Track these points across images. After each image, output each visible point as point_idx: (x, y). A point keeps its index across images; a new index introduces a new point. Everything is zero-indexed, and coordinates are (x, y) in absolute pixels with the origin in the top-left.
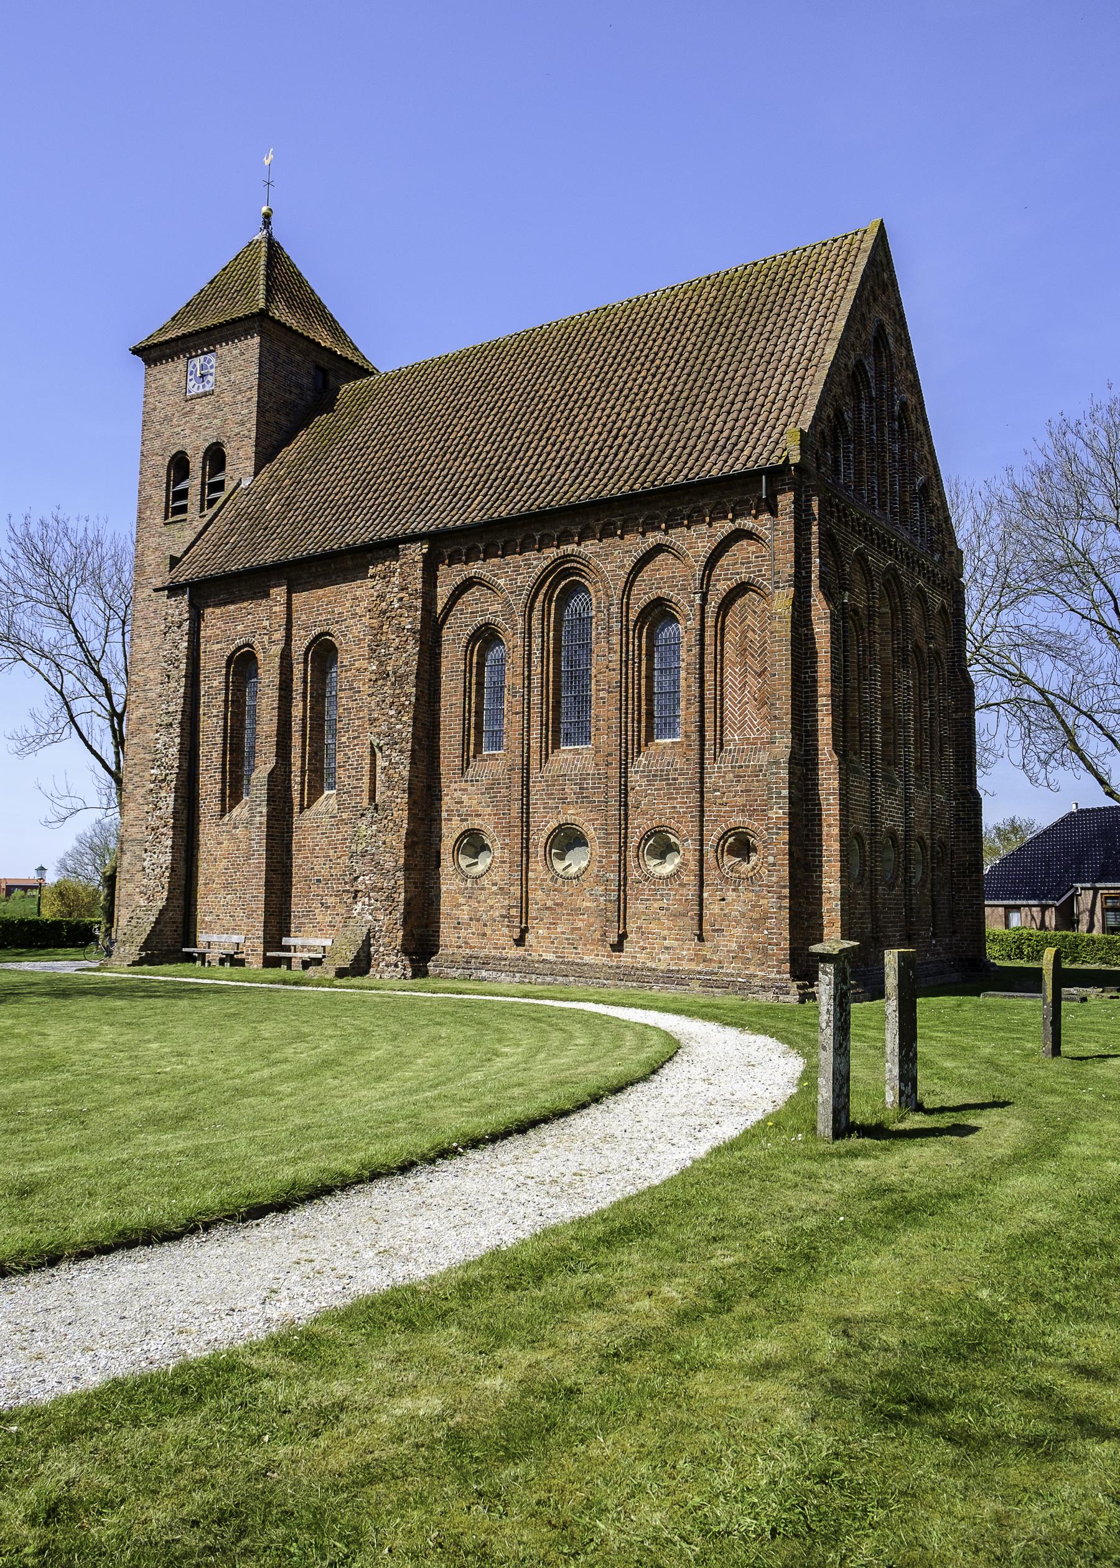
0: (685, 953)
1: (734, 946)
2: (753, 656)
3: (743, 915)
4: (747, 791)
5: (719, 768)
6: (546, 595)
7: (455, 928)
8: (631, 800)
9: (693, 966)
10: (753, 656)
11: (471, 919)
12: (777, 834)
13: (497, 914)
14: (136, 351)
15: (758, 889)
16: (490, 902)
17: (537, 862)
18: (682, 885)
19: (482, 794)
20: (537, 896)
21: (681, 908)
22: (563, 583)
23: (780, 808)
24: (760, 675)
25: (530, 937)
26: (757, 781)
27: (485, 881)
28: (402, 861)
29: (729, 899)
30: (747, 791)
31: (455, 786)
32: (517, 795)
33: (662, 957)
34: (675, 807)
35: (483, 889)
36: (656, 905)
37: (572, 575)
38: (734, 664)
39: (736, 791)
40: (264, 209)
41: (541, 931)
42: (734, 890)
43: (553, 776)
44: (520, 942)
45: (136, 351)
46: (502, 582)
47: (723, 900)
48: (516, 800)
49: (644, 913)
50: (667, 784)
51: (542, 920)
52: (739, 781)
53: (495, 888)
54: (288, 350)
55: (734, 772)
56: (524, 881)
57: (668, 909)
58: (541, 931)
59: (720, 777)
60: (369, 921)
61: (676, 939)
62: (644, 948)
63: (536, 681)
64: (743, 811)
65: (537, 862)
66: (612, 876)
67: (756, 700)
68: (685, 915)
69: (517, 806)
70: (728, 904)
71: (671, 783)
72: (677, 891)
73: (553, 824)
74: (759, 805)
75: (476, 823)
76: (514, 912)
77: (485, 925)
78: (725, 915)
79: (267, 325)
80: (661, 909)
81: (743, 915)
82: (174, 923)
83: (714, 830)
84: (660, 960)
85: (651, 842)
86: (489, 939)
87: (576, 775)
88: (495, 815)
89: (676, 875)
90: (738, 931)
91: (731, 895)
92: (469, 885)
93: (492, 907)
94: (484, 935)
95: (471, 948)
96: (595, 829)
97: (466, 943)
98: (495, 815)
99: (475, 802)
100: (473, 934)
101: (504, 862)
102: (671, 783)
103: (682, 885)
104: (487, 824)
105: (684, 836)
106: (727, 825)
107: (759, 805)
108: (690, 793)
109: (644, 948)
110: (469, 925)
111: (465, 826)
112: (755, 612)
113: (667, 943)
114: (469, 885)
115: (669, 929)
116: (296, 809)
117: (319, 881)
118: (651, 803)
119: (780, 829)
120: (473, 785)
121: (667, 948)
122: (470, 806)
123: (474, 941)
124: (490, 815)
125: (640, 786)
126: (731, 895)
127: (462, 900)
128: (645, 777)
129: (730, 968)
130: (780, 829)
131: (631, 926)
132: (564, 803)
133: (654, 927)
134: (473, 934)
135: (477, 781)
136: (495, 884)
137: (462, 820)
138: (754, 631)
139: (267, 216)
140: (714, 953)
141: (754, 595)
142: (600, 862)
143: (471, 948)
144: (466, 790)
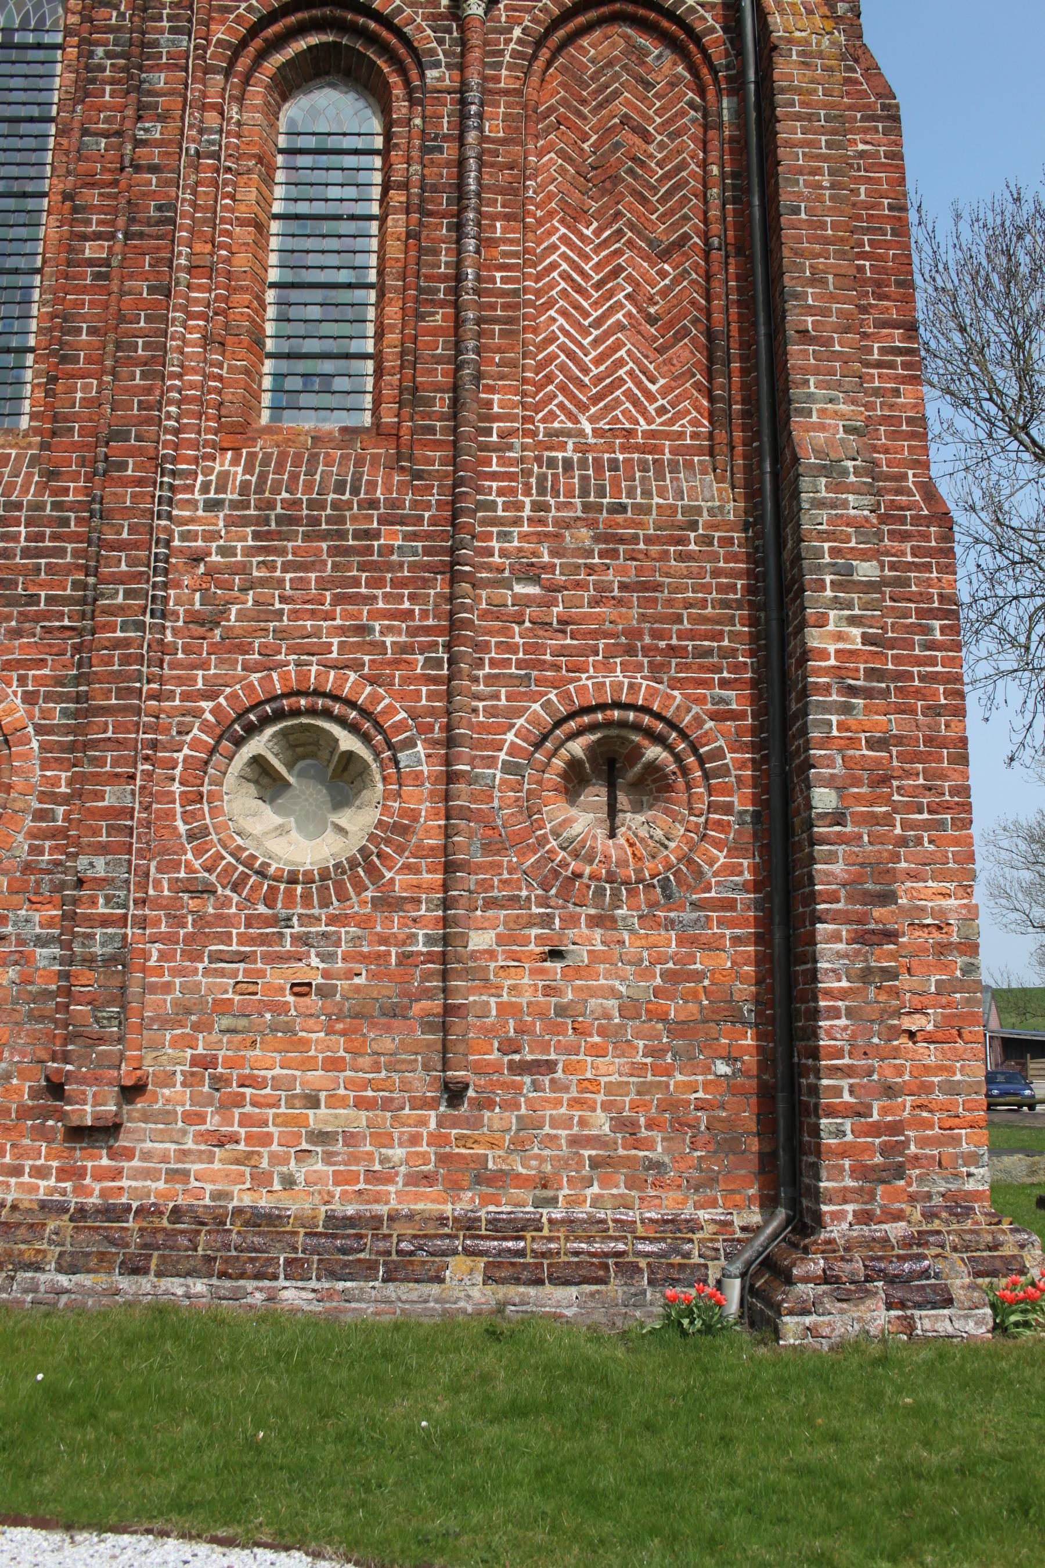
0: (398, 1153)
1: (601, 1123)
2: (644, 200)
3: (630, 1009)
4: (644, 587)
5: (537, 507)
8: (185, 597)
9: (430, 1203)
10: (644, 200)
12: (846, 709)
15: (688, 915)
18: (387, 903)
21: (388, 990)
23: (853, 621)
24: (665, 255)
26: (681, 557)
29: (581, 954)
30: (644, 587)
33: (299, 1172)
34: (363, 630)
36: (277, 977)
38: (575, 216)
39: (602, 587)
42: (602, 921)
47: (556, 954)
49: (223, 1007)
50: (333, 551)
52: (613, 554)
55: (592, 524)
57: (325, 992)
59: (542, 537)
61: (361, 1104)
62: (222, 1141)
64: (630, 651)
66: (100, 866)
67: (652, 320)
68: (395, 1012)
70: (578, 972)
71: (356, 551)
72: (364, 923)
74: (691, 635)
78: (562, 1010)
80: (301, 989)
81: (630, 1009)
83: (519, 712)
84: (289, 1182)
85: (259, 745)
89: (366, 864)
90: (610, 1069)
91: (585, 941)
96: (30, 698)
102: (356, 551)
103: (387, 903)
105: (400, 727)
106: (565, 697)
107: (691, 635)
108: (426, 583)
109: (222, 1141)
112: (648, 85)
113: (317, 1118)
115: (333, 1064)
118: (264, 612)
119: (853, 691)
121: (321, 1137)
125: (223, 551)
126: (585, 941)
128: (245, 521)
129: (591, 1199)
130: (853, 691)
131: (167, 1058)
133: (269, 1063)
138: (646, 137)
140: (519, 1146)
141: (643, 41)
142: (40, 815)
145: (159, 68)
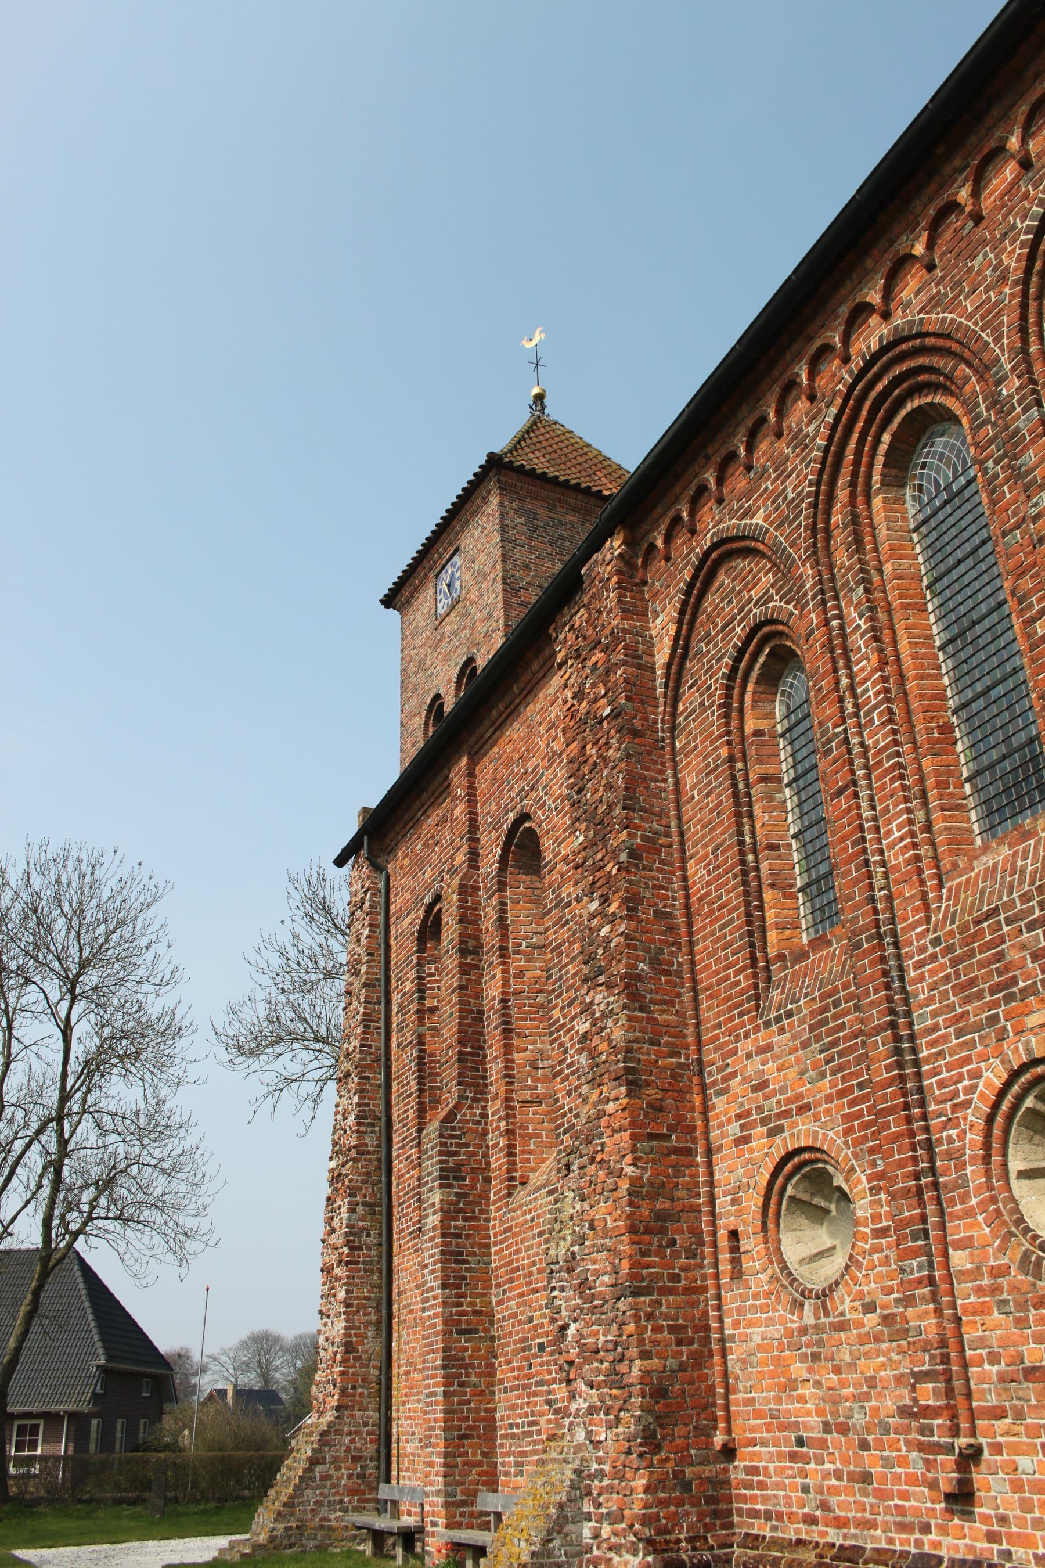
6: (853, 484)
7: (793, 1457)
11: (827, 1428)
13: (889, 1404)
14: (389, 601)
16: (868, 1366)
17: (970, 1213)
19: (806, 1045)
20: (988, 1330)
22: (886, 438)
25: (992, 1485)
27: (845, 1304)
28: (625, 1268)
31: (745, 1046)
32: (877, 1018)
35: (842, 1326)
37: (900, 403)
40: (536, 390)
41: (1024, 1462)
43: (964, 928)
44: (961, 1499)
45: (389, 601)
46: (758, 519)
48: (879, 1030)
51: (1019, 1416)
53: (871, 1320)
54: (551, 510)
56: (938, 1286)
58: (1024, 1462)
60: (578, 1448)
63: (870, 691)
65: (970, 1213)
69: (881, 1045)
73: (993, 1076)
75: (803, 1131)
76: (929, 1395)
77: (864, 1446)
79: (511, 478)
82: (356, 1459)
86: (882, 1495)
87: (1026, 898)
88: (841, 1094)
92: (809, 1319)
93: (871, 1382)
94: (866, 1478)
95: (841, 1523)
97: (824, 1506)
98: (841, 1094)
99: (792, 1073)
100: (838, 1475)
101: (883, 1232)
104: (821, 1130)
110: (823, 1444)
111: (781, 1145)
114: (809, 1319)
116: (497, 1186)
117: (541, 1347)
120: (782, 1031)
122: (783, 1090)
123: (846, 1502)
124: (829, 1099)
127: (798, 1369)
132: (1009, 998)
134: (838, 1475)
135: (789, 1014)
136: (870, 1308)
137: (773, 1133)
139: (540, 398)
143: (841, 1523)
144: (768, 1048)
145: (1026, 448)
